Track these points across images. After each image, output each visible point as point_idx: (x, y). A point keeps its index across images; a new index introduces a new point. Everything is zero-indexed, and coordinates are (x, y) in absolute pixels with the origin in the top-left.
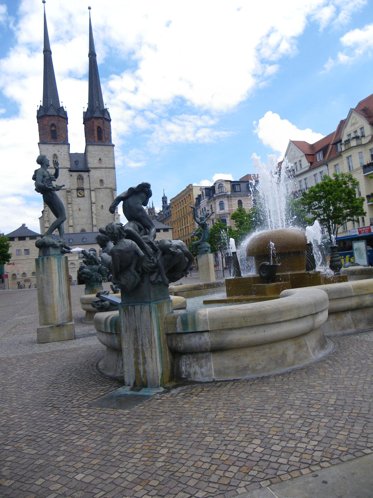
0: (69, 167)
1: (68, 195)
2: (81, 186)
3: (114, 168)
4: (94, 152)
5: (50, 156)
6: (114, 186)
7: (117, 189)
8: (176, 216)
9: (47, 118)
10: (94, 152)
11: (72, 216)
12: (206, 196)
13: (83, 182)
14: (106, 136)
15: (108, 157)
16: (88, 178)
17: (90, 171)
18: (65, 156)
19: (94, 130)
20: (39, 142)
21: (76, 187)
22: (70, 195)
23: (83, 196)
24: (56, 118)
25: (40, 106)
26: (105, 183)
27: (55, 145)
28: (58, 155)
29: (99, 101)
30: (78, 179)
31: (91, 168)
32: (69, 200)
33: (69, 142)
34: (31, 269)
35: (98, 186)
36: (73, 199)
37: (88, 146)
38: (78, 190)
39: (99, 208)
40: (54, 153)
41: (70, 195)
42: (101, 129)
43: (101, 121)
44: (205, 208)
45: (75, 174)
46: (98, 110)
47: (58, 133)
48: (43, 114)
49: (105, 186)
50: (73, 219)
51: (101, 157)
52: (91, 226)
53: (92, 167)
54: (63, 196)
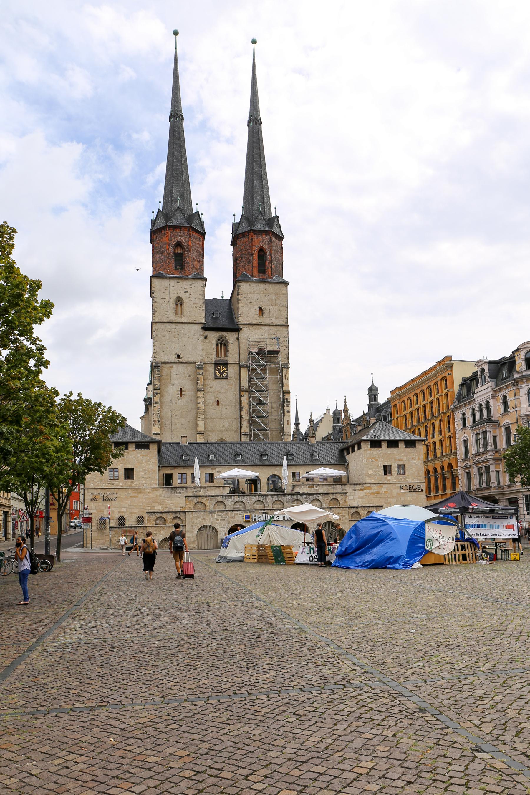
0: (203, 321)
1: (198, 374)
4: (250, 295)
5: (171, 301)
6: (284, 360)
7: (290, 366)
8: (404, 422)
9: (170, 233)
10: (250, 295)
12: (490, 377)
13: (226, 351)
14: (273, 266)
16: (237, 343)
17: (241, 329)
18: (197, 301)
19: (252, 255)
20: (151, 275)
21: (213, 358)
22: (203, 373)
23: (227, 378)
24: (186, 232)
25: (159, 211)
27: (179, 281)
28: (185, 299)
29: (263, 203)
30: (217, 345)
31: (244, 324)
33: (205, 276)
34: (135, 510)
36: (207, 382)
38: (216, 364)
40: (177, 295)
41: (203, 373)
42: (265, 253)
44: (488, 403)
45: (213, 336)
46: (260, 217)
47: (187, 259)
48: (162, 225)
50: (205, 419)
51: (261, 303)
52: (238, 435)
53: (246, 322)
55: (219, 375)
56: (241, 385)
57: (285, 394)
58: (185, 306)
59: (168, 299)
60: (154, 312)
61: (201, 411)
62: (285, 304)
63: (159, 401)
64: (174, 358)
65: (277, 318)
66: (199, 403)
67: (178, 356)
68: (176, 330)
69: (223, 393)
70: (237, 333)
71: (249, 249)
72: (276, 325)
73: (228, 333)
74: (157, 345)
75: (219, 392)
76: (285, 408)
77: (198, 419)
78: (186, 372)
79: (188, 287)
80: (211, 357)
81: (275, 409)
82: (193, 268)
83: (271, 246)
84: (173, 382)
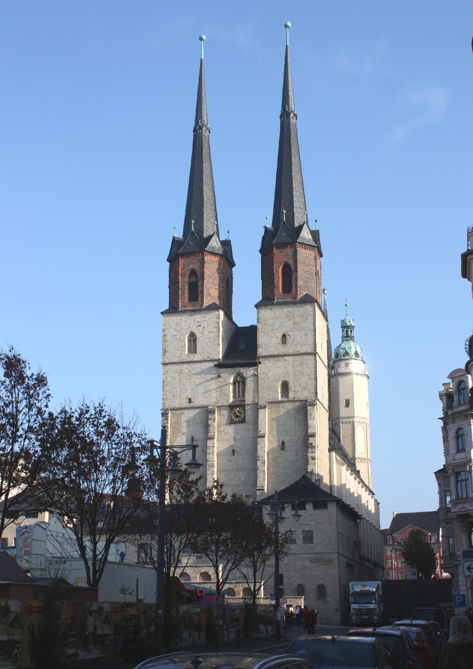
23: (243, 421)
27: (192, 314)
28: (198, 335)
51: (285, 329)
54: (201, 423)
61: (210, 463)
64: (185, 403)
66: (209, 454)
67: (190, 399)
69: (239, 440)
72: (302, 354)
76: (310, 455)
82: (209, 298)
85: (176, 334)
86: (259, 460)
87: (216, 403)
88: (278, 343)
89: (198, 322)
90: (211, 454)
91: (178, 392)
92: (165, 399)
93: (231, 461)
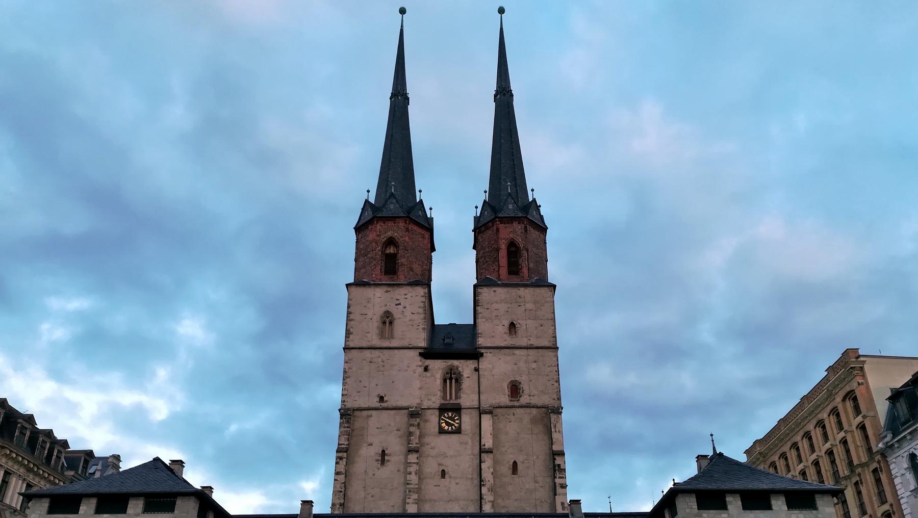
0: (423, 344)
1: (412, 425)
2: (452, 402)
3: (555, 348)
6: (553, 402)
9: (379, 226)
10: (495, 306)
11: (418, 490)
13: (459, 389)
15: (536, 318)
17: (482, 355)
18: (415, 317)
21: (436, 400)
22: (419, 424)
23: (458, 431)
24: (402, 224)
26: (527, 391)
27: (389, 289)
28: (396, 316)
30: (445, 381)
32: (415, 440)
35: (504, 399)
37: (479, 290)
38: (442, 410)
39: (506, 469)
40: (384, 309)
41: (419, 424)
42: (518, 248)
43: (518, 227)
45: (438, 366)
49: (524, 400)
53: (489, 345)
54: (398, 430)
55: (446, 428)
56: (482, 443)
57: (556, 457)
58: (396, 323)
59: (370, 315)
60: (348, 333)
61: (412, 486)
62: (550, 316)
63: (343, 471)
64: (375, 402)
65: (537, 337)
66: (410, 473)
67: (382, 399)
68: (380, 360)
69: (451, 457)
70: (476, 361)
71: (494, 244)
72: (537, 348)
73: (462, 361)
74: (348, 383)
75: (445, 456)
76: (558, 481)
77: (408, 501)
78: (392, 424)
79: (401, 298)
80: (433, 399)
81: (541, 484)
82: (411, 273)
83: (526, 237)
84: (370, 441)
85: (366, 313)
86: (483, 485)
87: (419, 404)
88: (505, 333)
89: (397, 299)
90: (413, 474)
91: (365, 387)
92: (346, 395)
93: (439, 486)
